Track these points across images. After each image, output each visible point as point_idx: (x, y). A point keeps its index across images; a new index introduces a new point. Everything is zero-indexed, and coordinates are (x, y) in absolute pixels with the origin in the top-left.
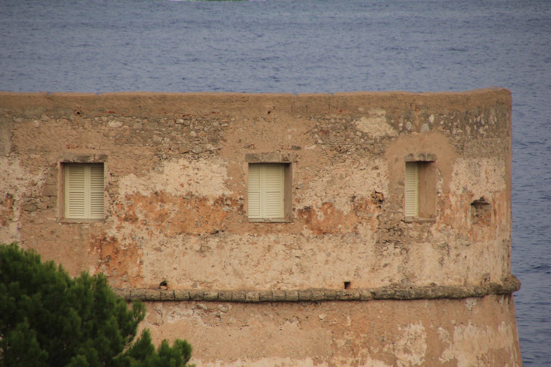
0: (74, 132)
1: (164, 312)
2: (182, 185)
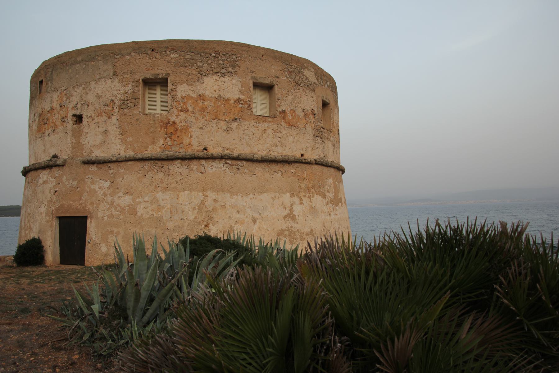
0: (150, 61)
1: (206, 165)
2: (215, 91)
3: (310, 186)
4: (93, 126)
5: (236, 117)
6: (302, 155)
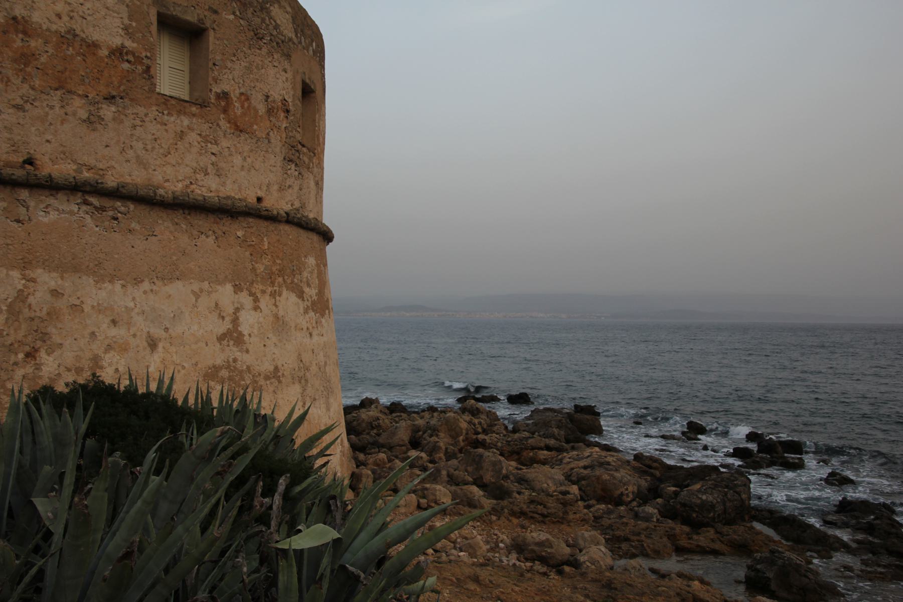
1: (32, 204)
3: (274, 269)
5: (114, 93)
6: (259, 200)
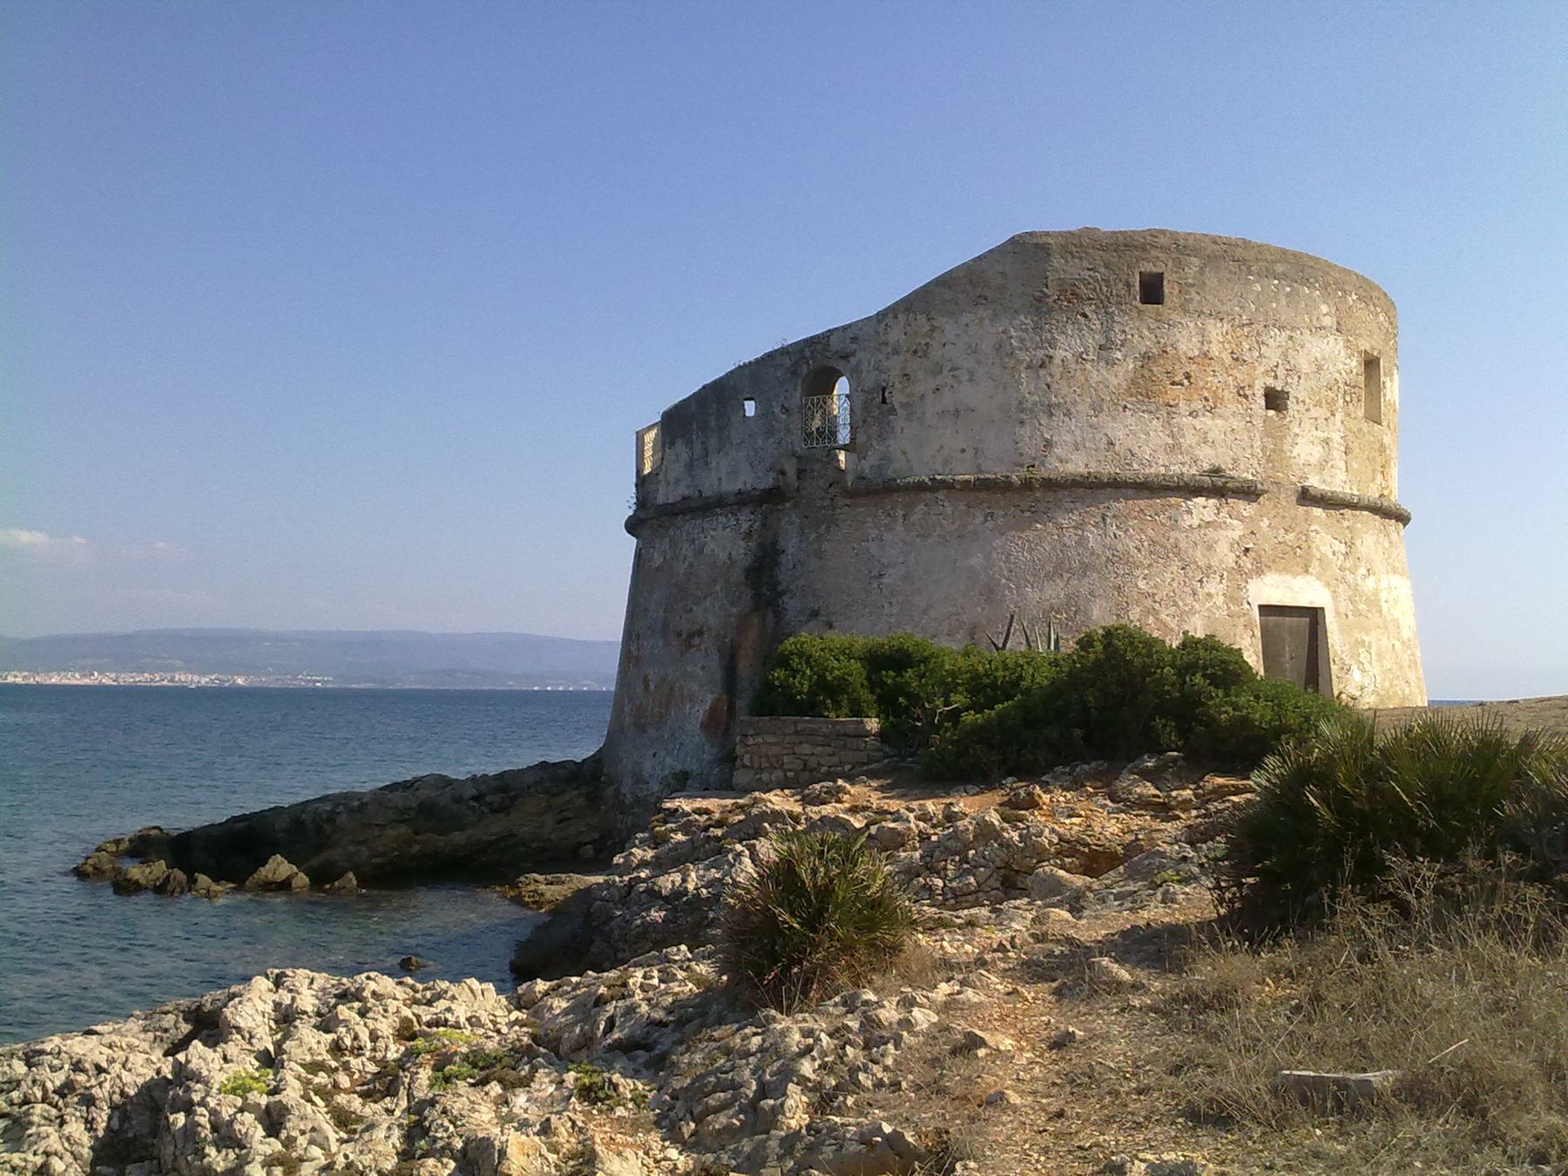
4: (1307, 424)
